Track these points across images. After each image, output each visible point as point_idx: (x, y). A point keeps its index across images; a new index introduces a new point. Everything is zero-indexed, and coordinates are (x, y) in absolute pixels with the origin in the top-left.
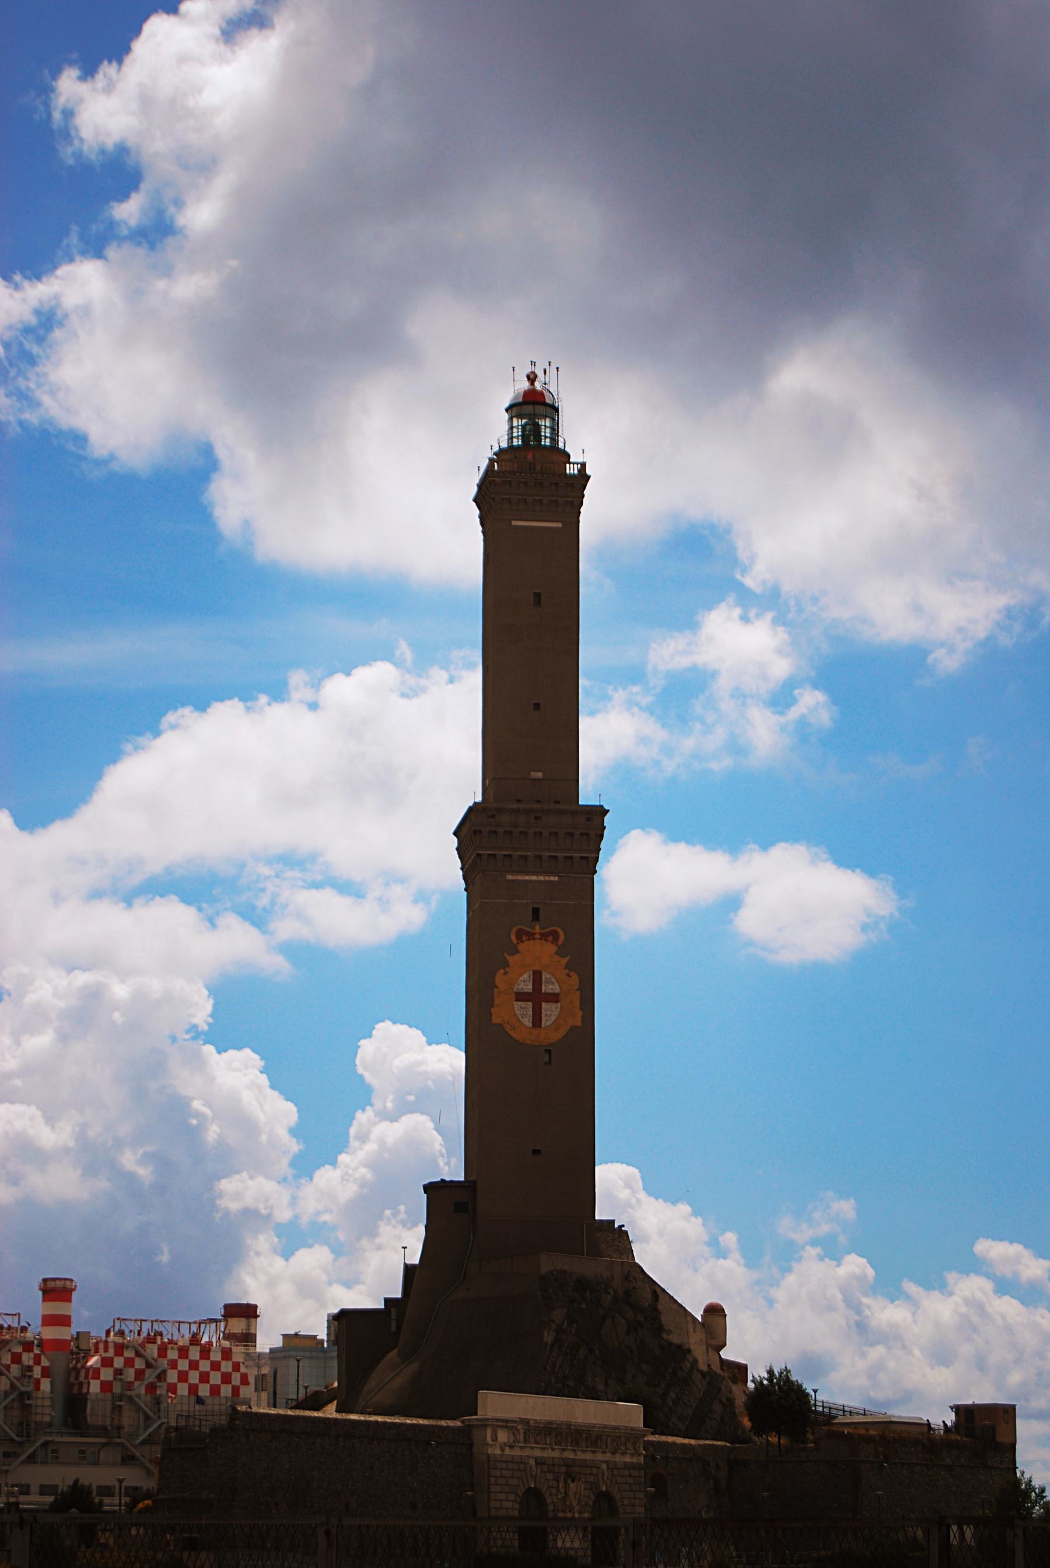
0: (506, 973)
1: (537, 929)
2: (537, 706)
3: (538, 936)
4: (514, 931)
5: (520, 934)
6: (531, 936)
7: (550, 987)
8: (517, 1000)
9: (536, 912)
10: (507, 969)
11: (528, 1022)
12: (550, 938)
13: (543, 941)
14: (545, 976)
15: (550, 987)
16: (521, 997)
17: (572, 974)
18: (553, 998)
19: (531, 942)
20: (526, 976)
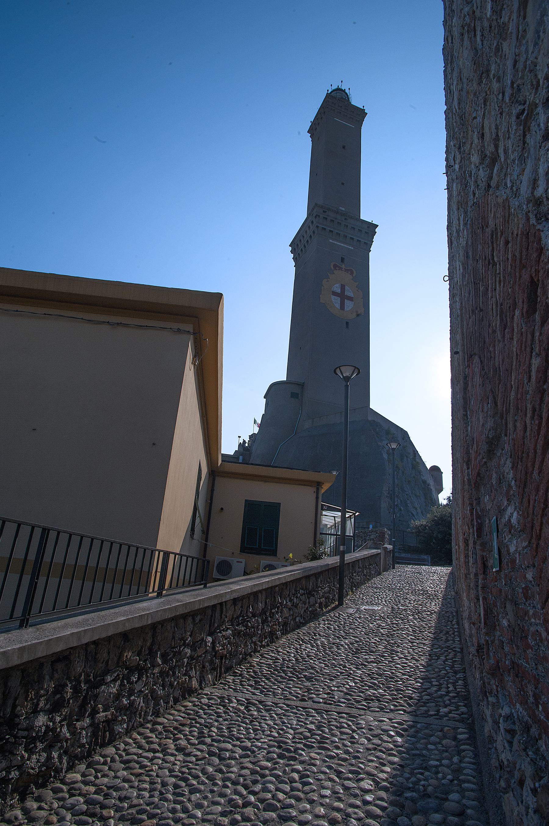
1: (343, 266)
4: (332, 264)
5: (335, 266)
6: (341, 269)
7: (349, 293)
9: (343, 260)
11: (338, 306)
14: (346, 288)
16: (334, 294)
17: (359, 290)
18: (350, 299)
20: (337, 285)
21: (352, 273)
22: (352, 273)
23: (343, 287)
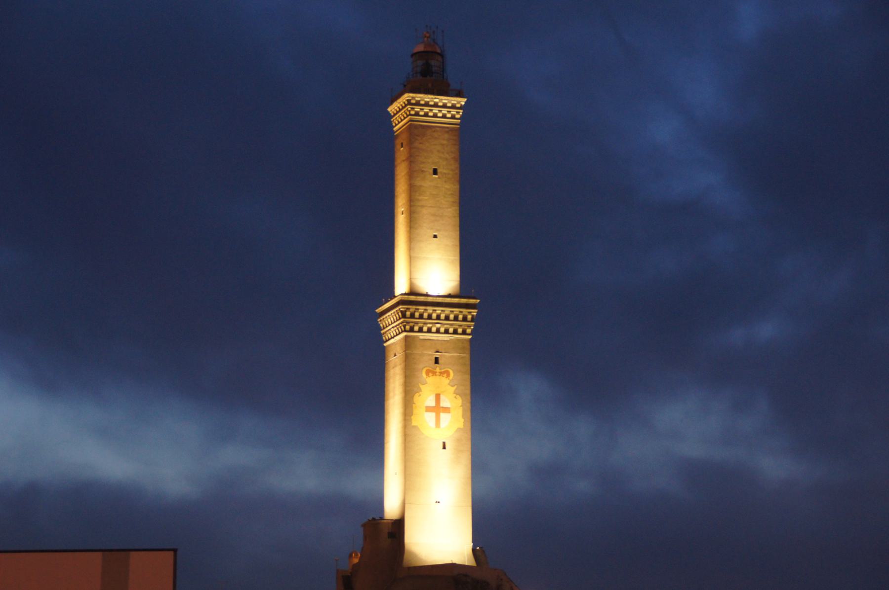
1: (438, 370)
2: (435, 236)
6: (434, 373)
9: (437, 361)
14: (442, 397)
15: (445, 403)
18: (447, 410)
21: (448, 375)
23: (438, 397)
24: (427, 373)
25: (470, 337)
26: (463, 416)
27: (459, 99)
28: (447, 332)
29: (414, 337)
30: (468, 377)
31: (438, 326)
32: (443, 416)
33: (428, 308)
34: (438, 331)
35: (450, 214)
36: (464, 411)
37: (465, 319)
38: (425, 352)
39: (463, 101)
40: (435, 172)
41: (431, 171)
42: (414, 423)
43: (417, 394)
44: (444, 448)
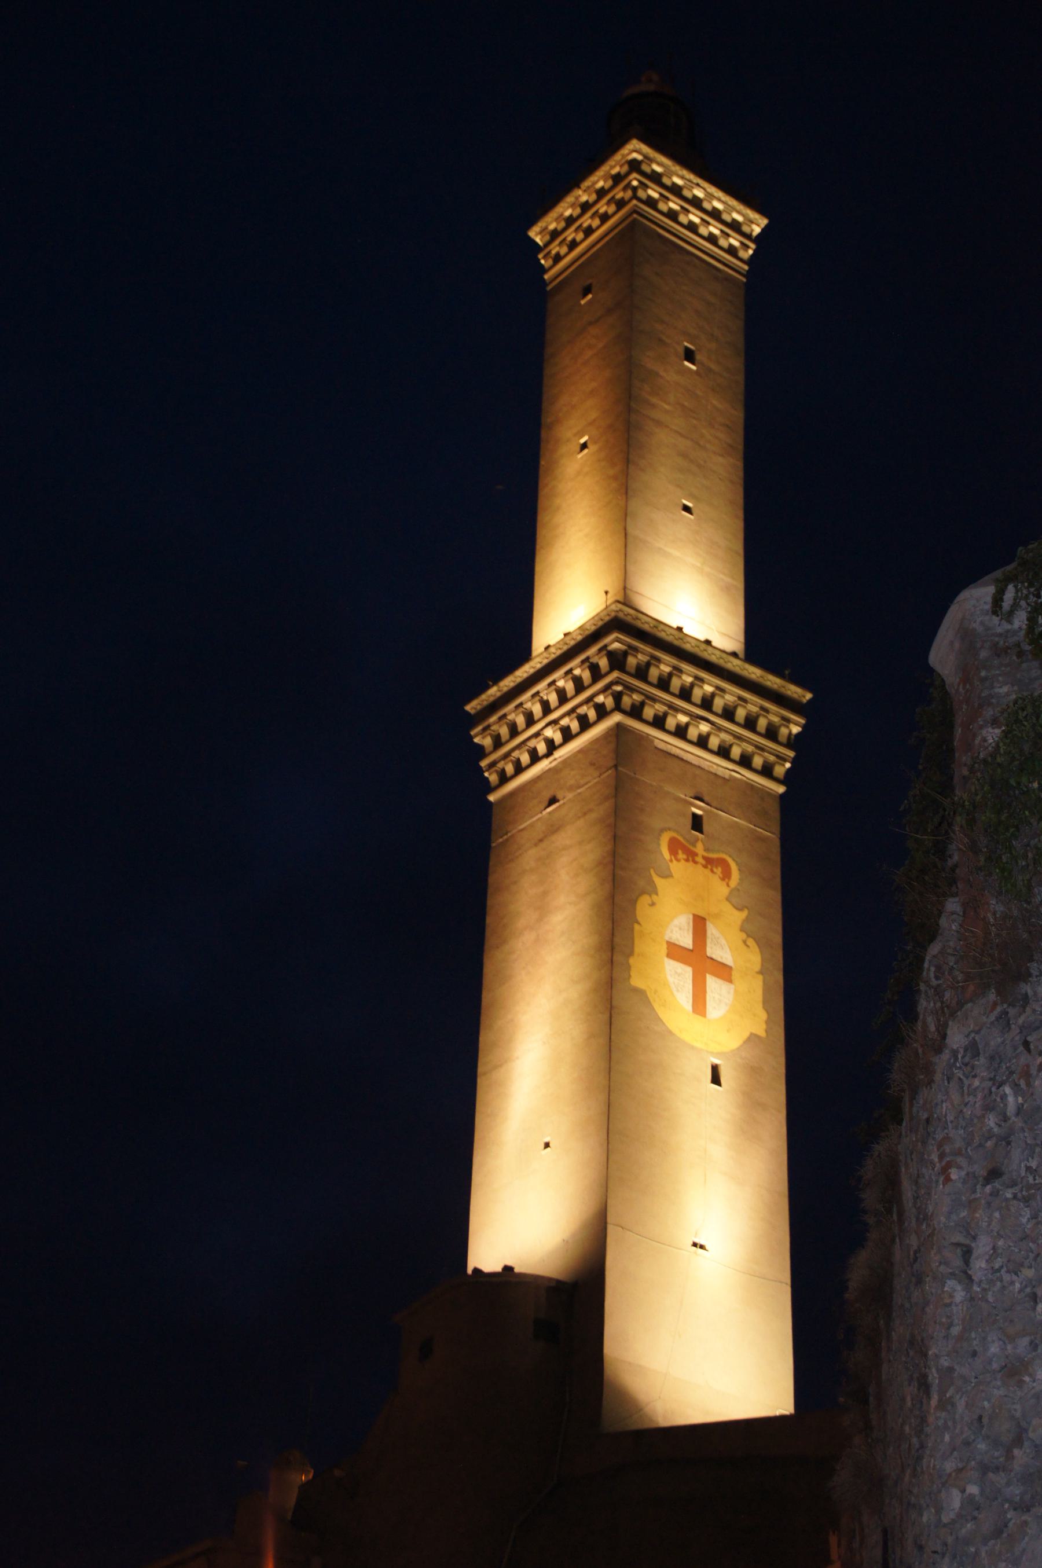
0: (653, 904)
3: (699, 859)
6: (691, 856)
8: (670, 955)
9: (697, 823)
10: (654, 897)
12: (719, 871)
13: (707, 872)
14: (711, 930)
17: (751, 942)
18: (724, 972)
19: (690, 864)
21: (726, 875)
22: (726, 875)
24: (675, 846)
25: (781, 789)
26: (766, 1003)
27: (752, 215)
28: (724, 752)
29: (642, 739)
30: (775, 896)
31: (704, 728)
32: (713, 985)
33: (685, 666)
34: (702, 742)
35: (723, 470)
36: (767, 989)
37: (771, 733)
38: (668, 788)
39: (757, 225)
40: (689, 356)
41: (681, 351)
42: (636, 981)
43: (644, 900)
44: (716, 1079)
